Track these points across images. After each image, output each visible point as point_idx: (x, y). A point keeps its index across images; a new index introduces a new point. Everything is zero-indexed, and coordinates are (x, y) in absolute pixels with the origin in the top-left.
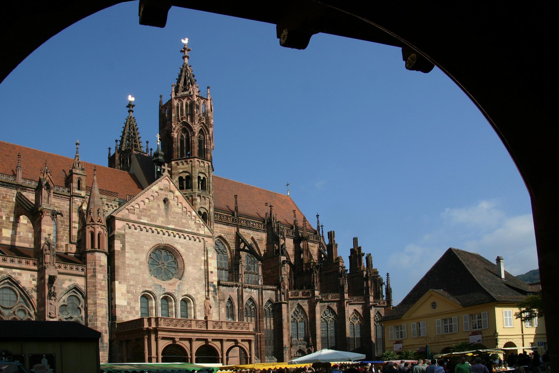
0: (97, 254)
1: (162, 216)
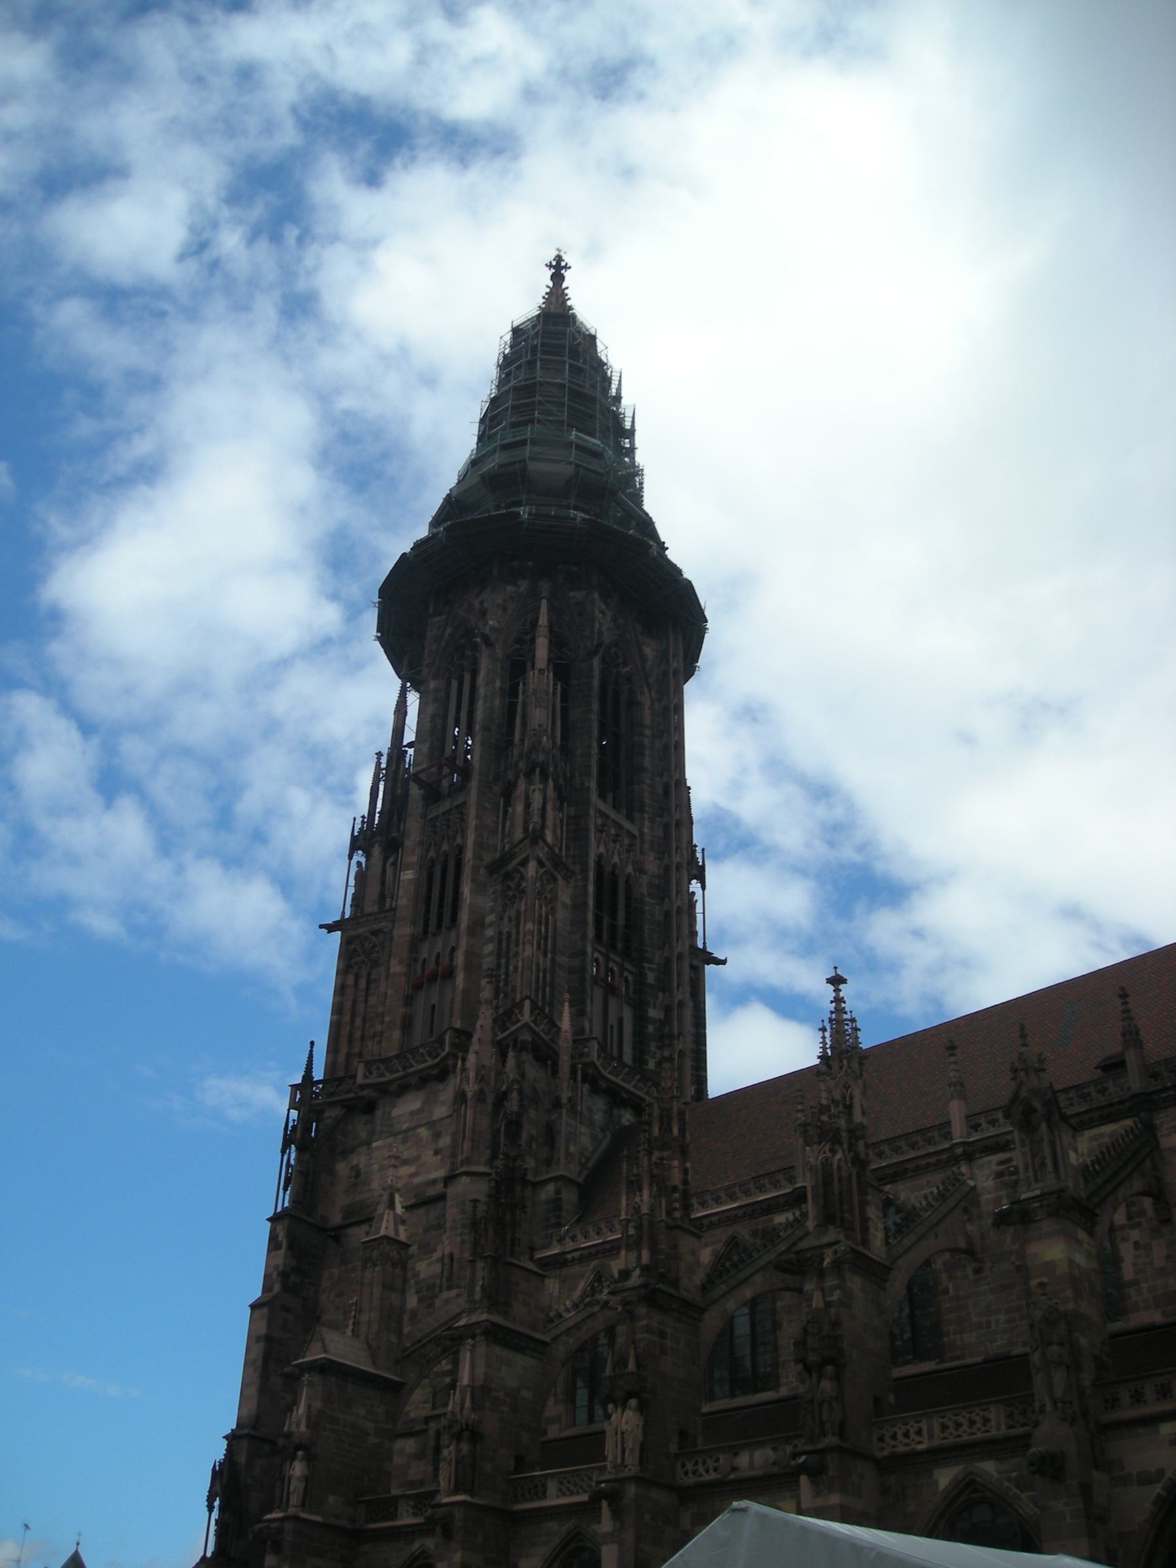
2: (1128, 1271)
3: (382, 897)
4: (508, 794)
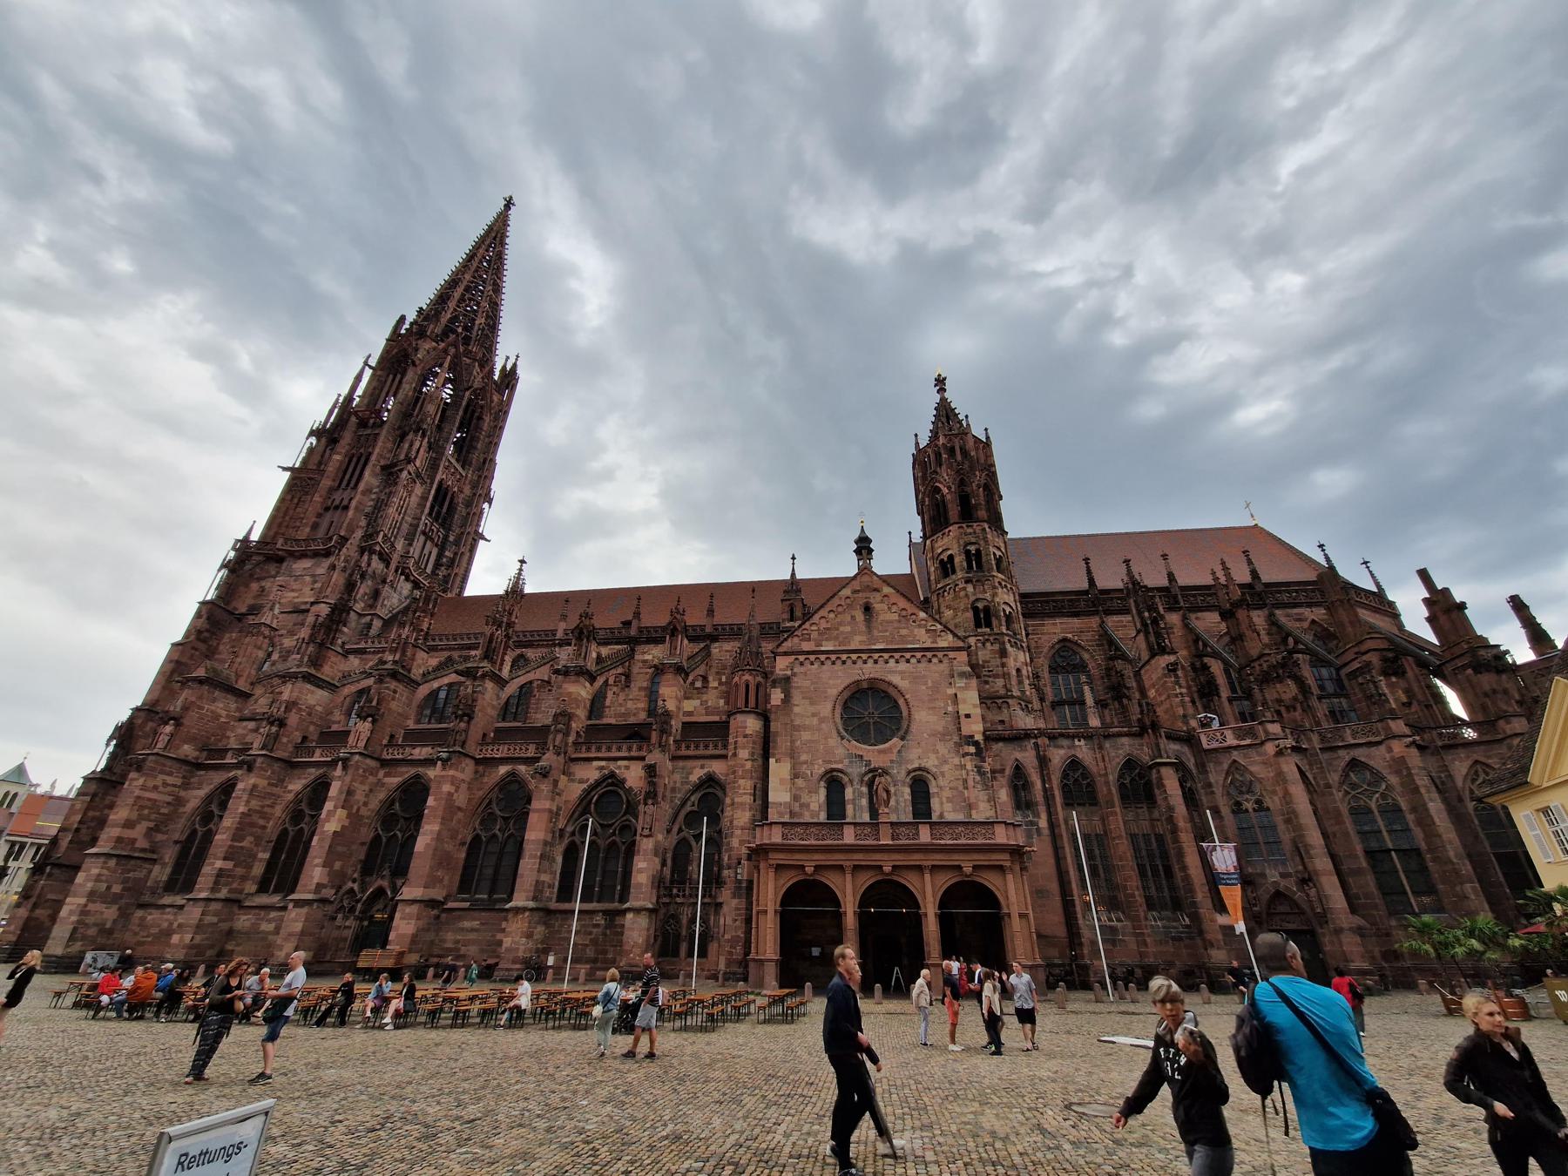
0: (740, 717)
1: (860, 633)
2: (608, 702)
3: (320, 463)
4: (403, 437)
